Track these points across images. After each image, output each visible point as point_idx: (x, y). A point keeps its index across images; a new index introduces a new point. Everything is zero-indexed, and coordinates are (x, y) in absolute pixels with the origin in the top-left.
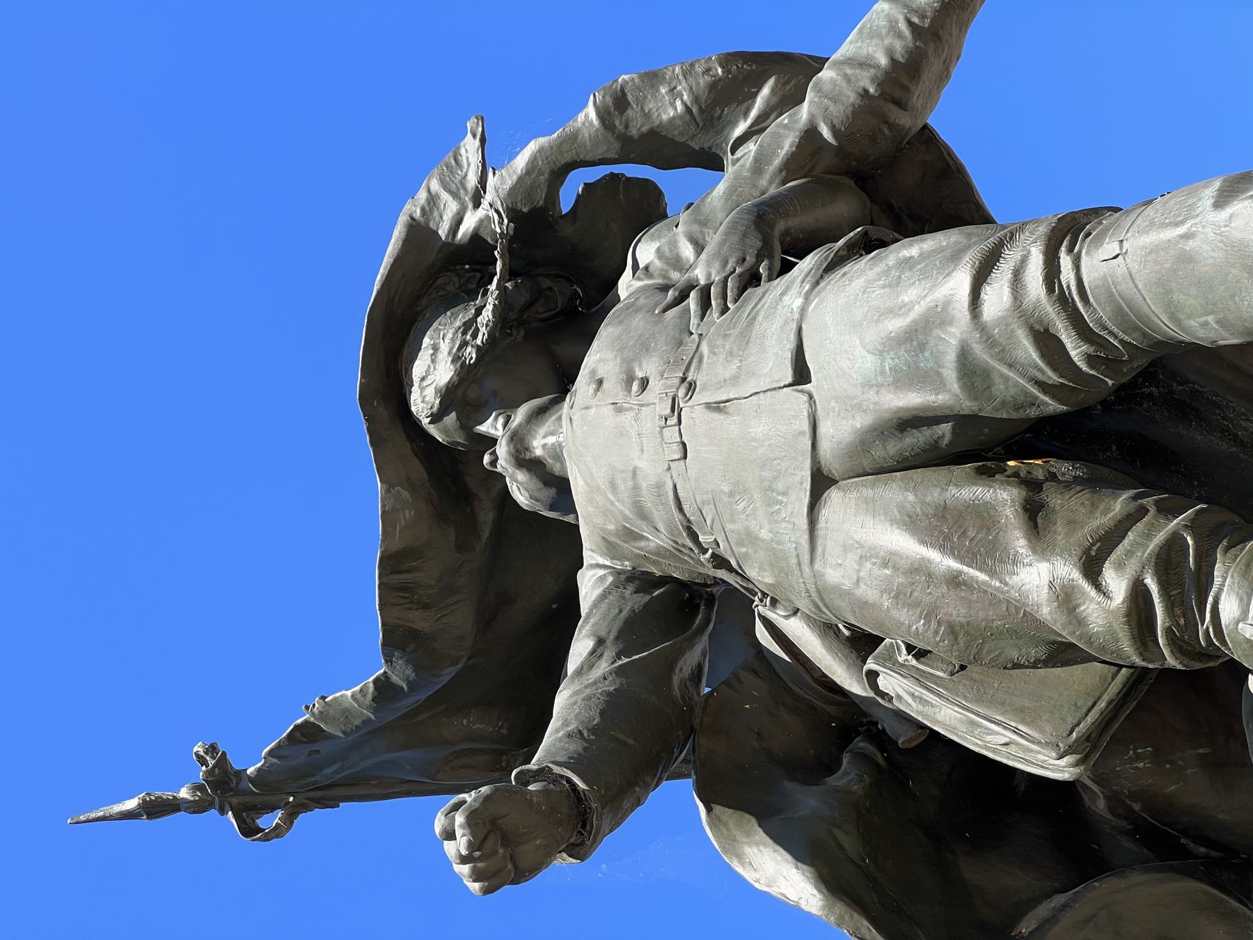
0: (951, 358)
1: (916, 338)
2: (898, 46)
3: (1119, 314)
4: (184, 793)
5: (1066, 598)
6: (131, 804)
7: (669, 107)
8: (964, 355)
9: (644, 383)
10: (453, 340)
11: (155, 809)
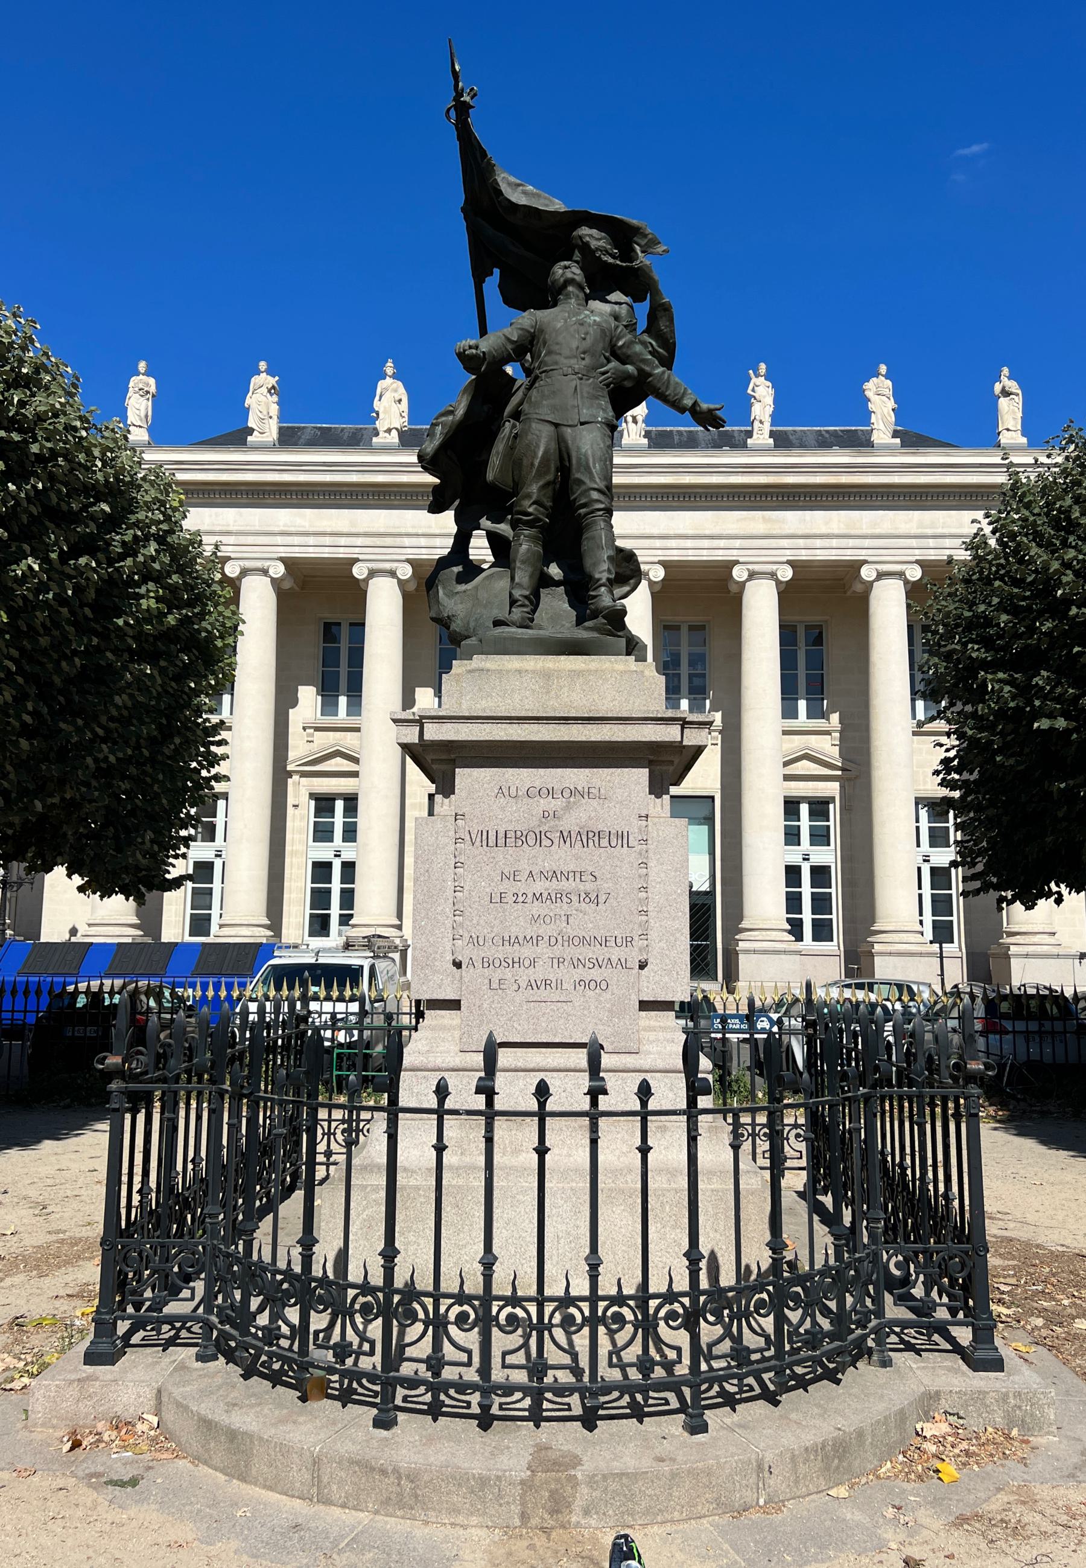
0: (583, 478)
1: (588, 469)
3: (588, 525)
4: (460, 84)
5: (528, 496)
6: (457, 68)
7: (663, 325)
9: (583, 359)
11: (455, 75)
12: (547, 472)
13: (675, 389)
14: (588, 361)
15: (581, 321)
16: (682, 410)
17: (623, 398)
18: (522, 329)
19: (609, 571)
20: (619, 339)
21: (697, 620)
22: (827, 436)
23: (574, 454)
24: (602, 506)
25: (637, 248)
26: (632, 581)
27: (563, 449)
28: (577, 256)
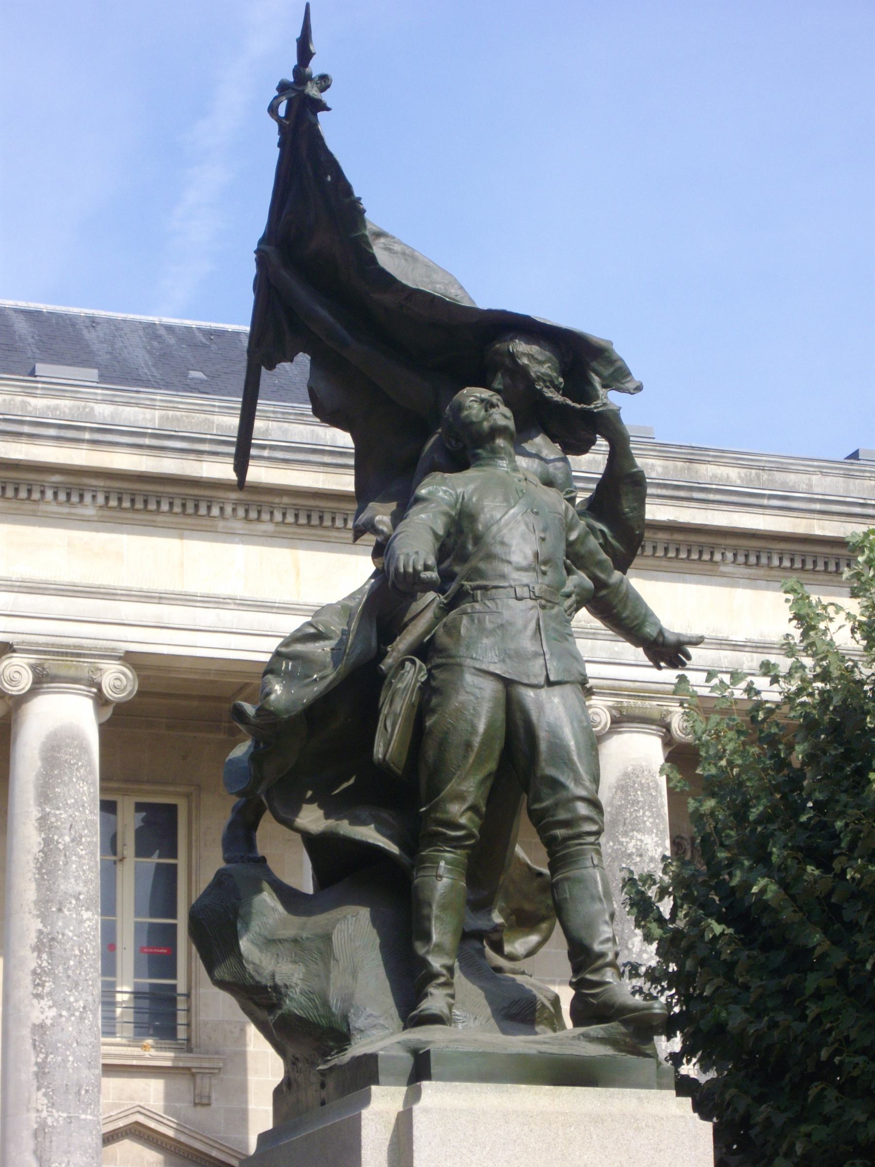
0: (562, 779)
2: (628, 621)
8: (563, 786)
9: (544, 573)
15: (520, 502)
22: (172, 340)
23: (542, 734)
25: (597, 381)
26: (544, 926)
27: (520, 723)
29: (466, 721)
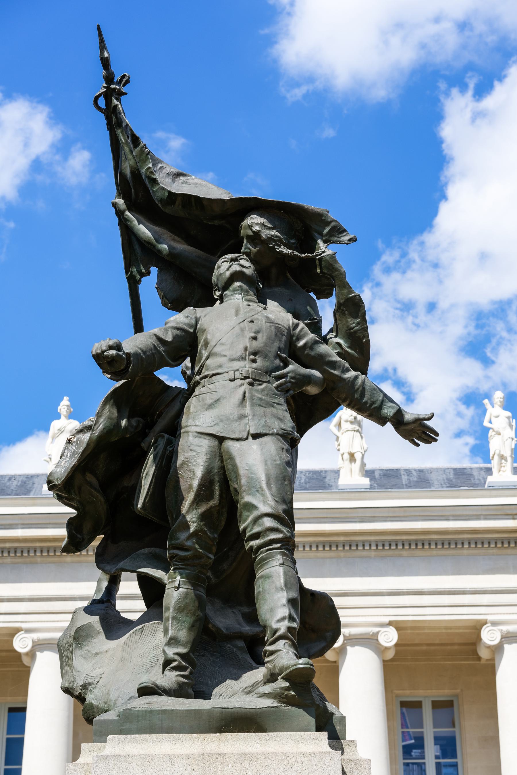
0: (255, 502)
9: (254, 361)
10: (277, 236)
12: (210, 497)
13: (372, 395)
14: (260, 363)
16: (382, 421)
17: (308, 409)
18: (178, 329)
19: (291, 618)
20: (299, 339)
21: (443, 694)
24: (280, 536)
28: (246, 245)
29: (190, 471)
